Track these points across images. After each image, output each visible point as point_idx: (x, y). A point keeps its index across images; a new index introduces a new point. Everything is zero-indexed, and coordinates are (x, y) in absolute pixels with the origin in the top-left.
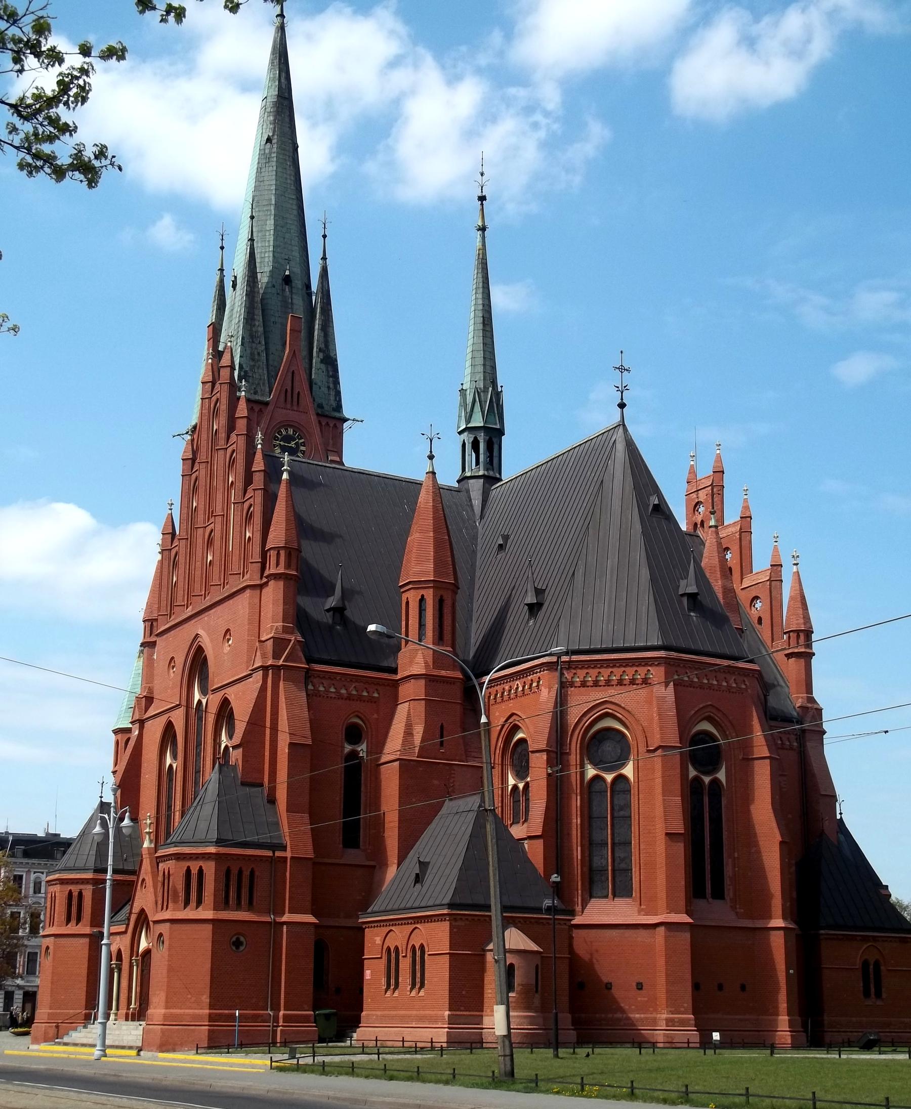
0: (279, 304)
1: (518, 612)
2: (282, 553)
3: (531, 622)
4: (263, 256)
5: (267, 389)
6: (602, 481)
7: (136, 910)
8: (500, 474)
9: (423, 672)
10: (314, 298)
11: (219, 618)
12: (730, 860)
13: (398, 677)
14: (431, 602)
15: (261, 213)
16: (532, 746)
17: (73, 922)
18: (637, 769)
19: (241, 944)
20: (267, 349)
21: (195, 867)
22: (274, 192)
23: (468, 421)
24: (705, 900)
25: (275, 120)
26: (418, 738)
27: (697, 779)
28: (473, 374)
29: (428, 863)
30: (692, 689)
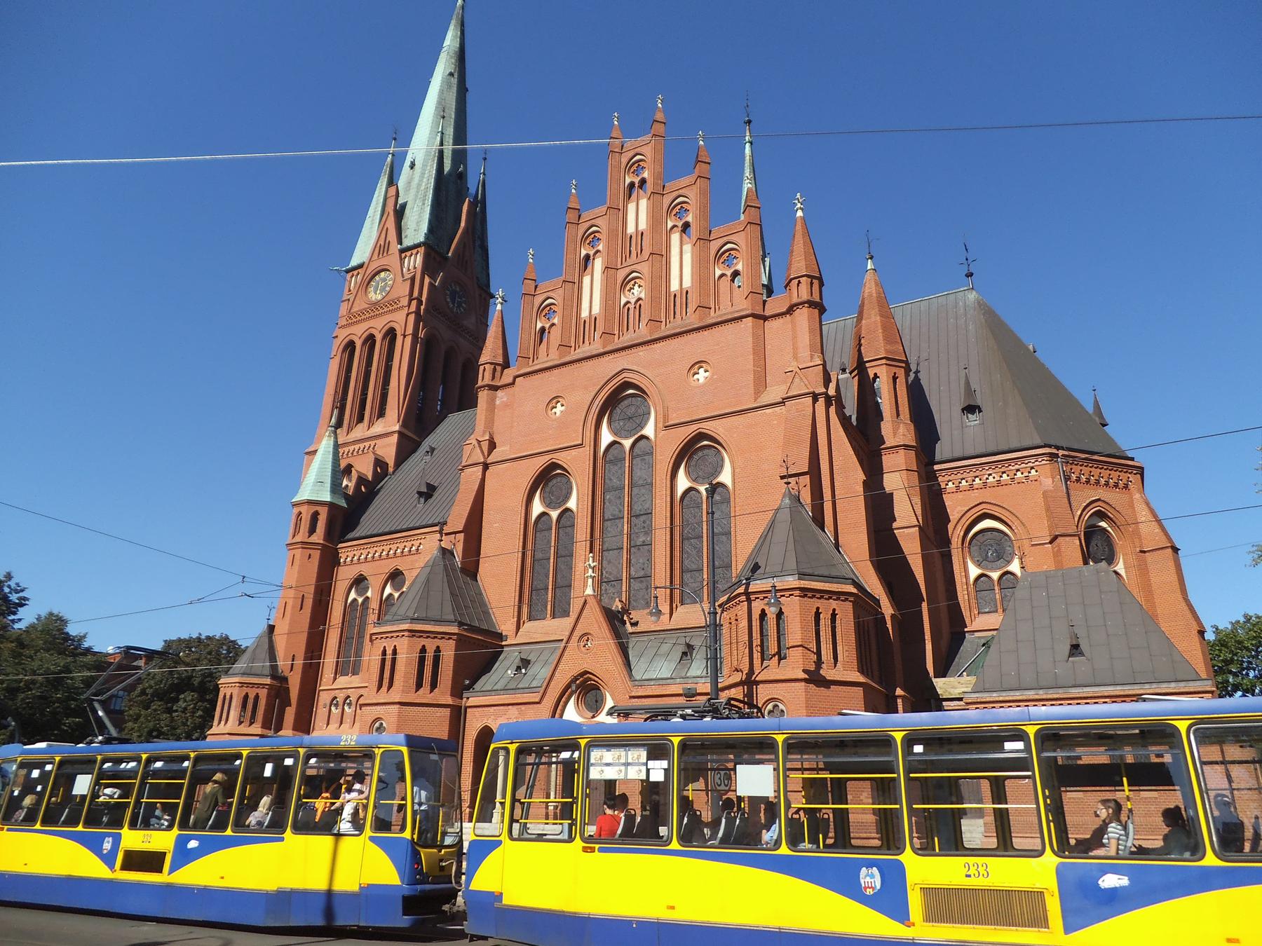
2: (803, 280)
21: (431, 645)
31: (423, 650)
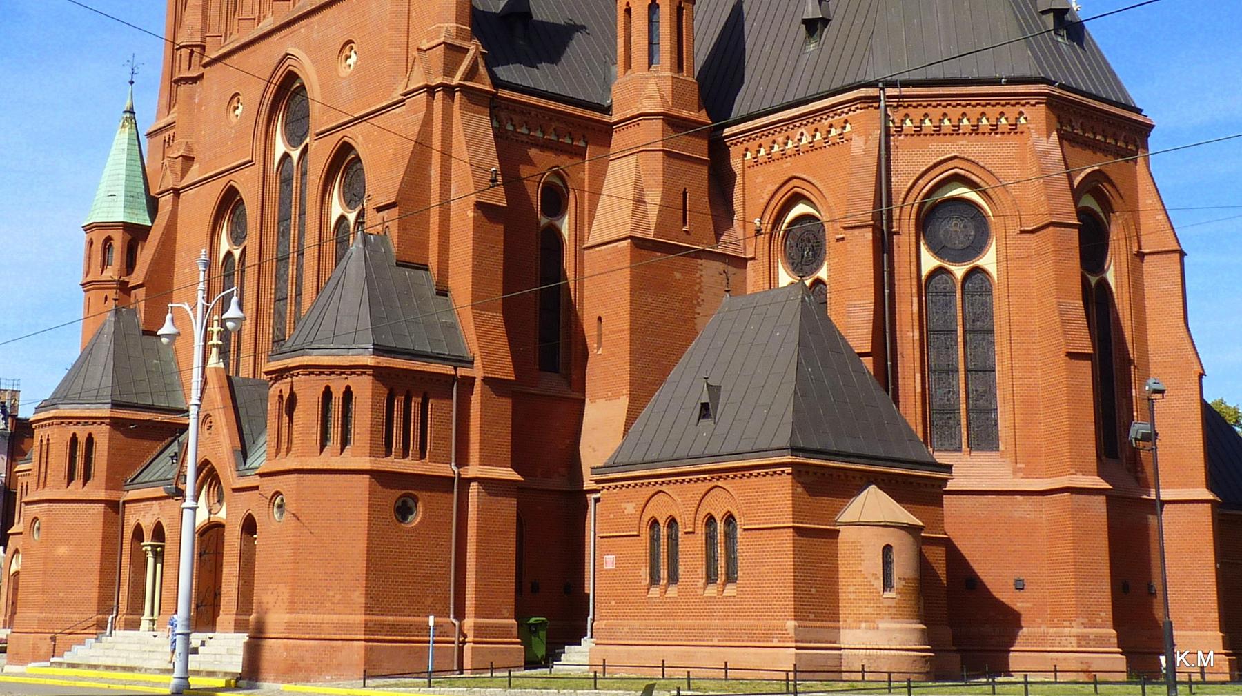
3: (812, 47)
9: (660, 110)
13: (613, 119)
14: (668, 8)
18: (1004, 259)
26: (653, 211)
31: (74, 440)
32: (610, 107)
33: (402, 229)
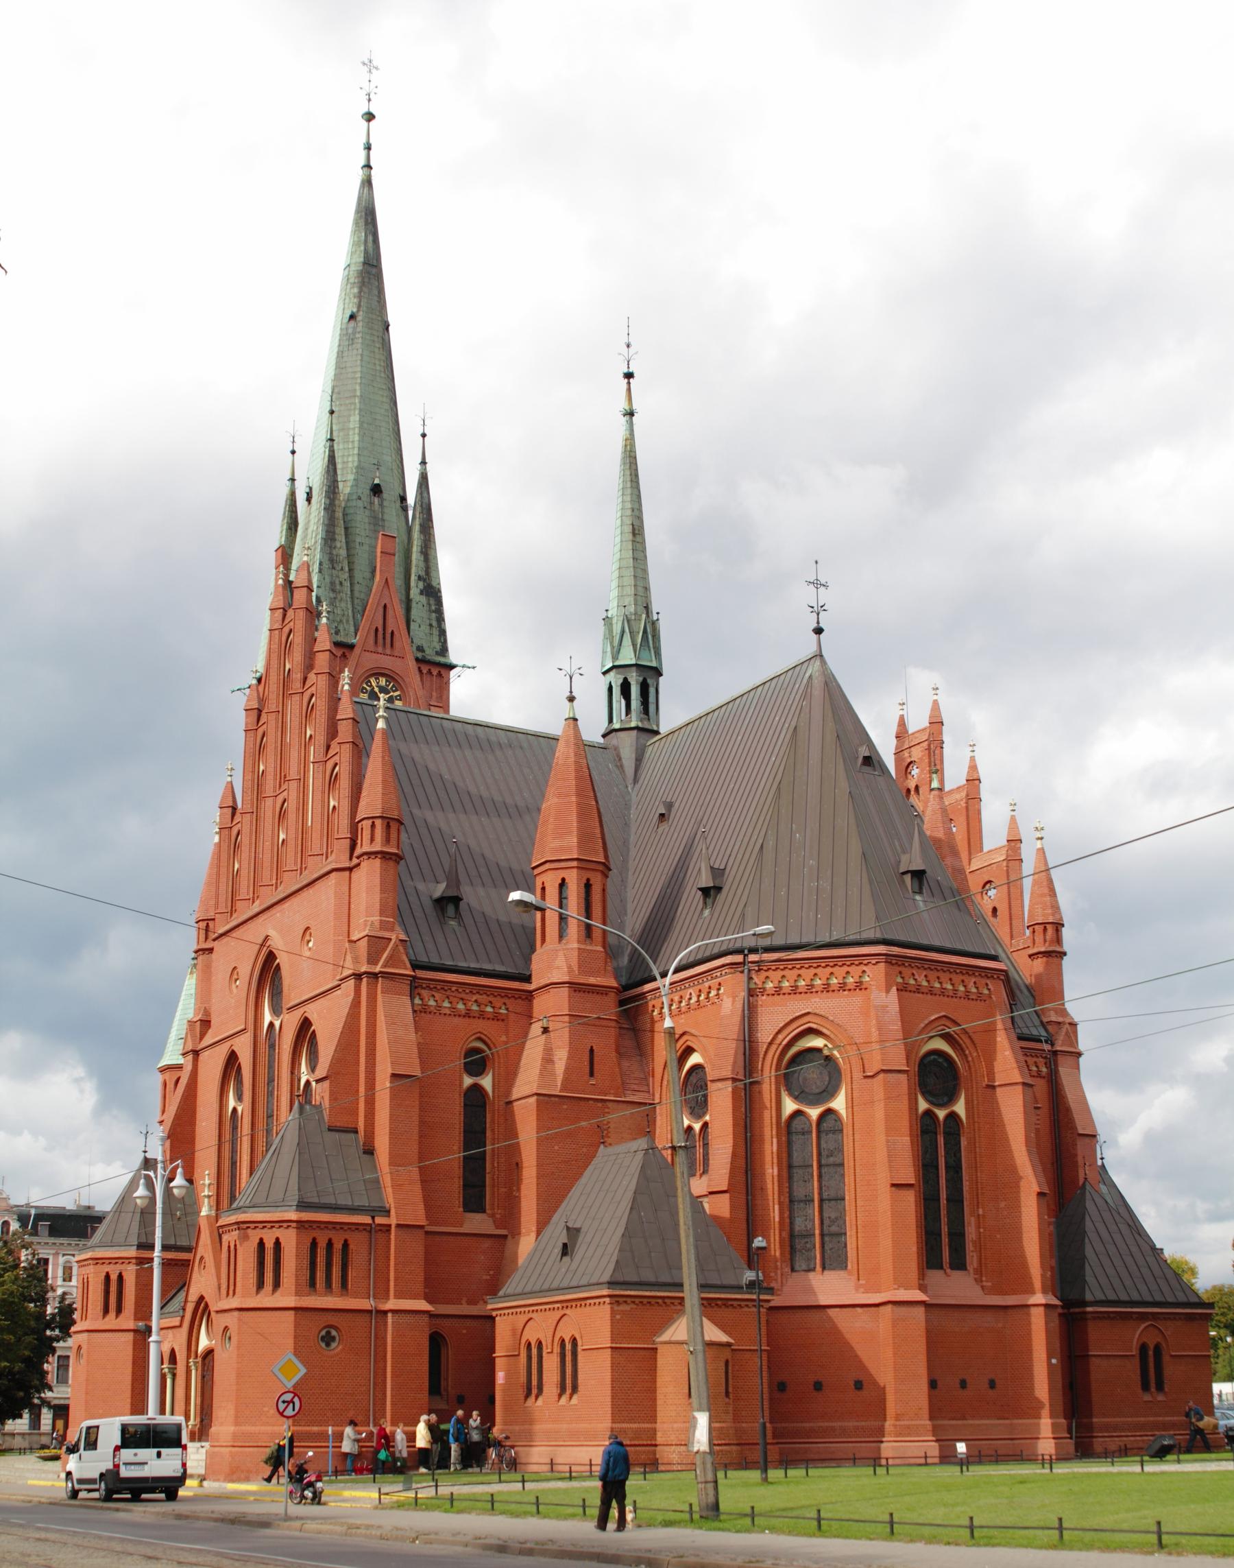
0: (367, 520)
1: (691, 898)
2: (378, 822)
3: (707, 912)
4: (345, 460)
5: (352, 629)
6: (796, 728)
7: (193, 1297)
8: (658, 725)
9: (566, 979)
10: (410, 513)
11: (294, 914)
12: (973, 1219)
13: (532, 987)
15: (342, 408)
16: (711, 1074)
17: (112, 1314)
19: (333, 1339)
20: (351, 577)
22: (359, 381)
23: (615, 658)
24: (941, 1272)
25: (360, 292)
26: (560, 1066)
27: (928, 1113)
28: (620, 597)
29: (578, 1230)
30: (920, 995)
31: (107, 1276)
32: (530, 976)
33: (334, 1097)
